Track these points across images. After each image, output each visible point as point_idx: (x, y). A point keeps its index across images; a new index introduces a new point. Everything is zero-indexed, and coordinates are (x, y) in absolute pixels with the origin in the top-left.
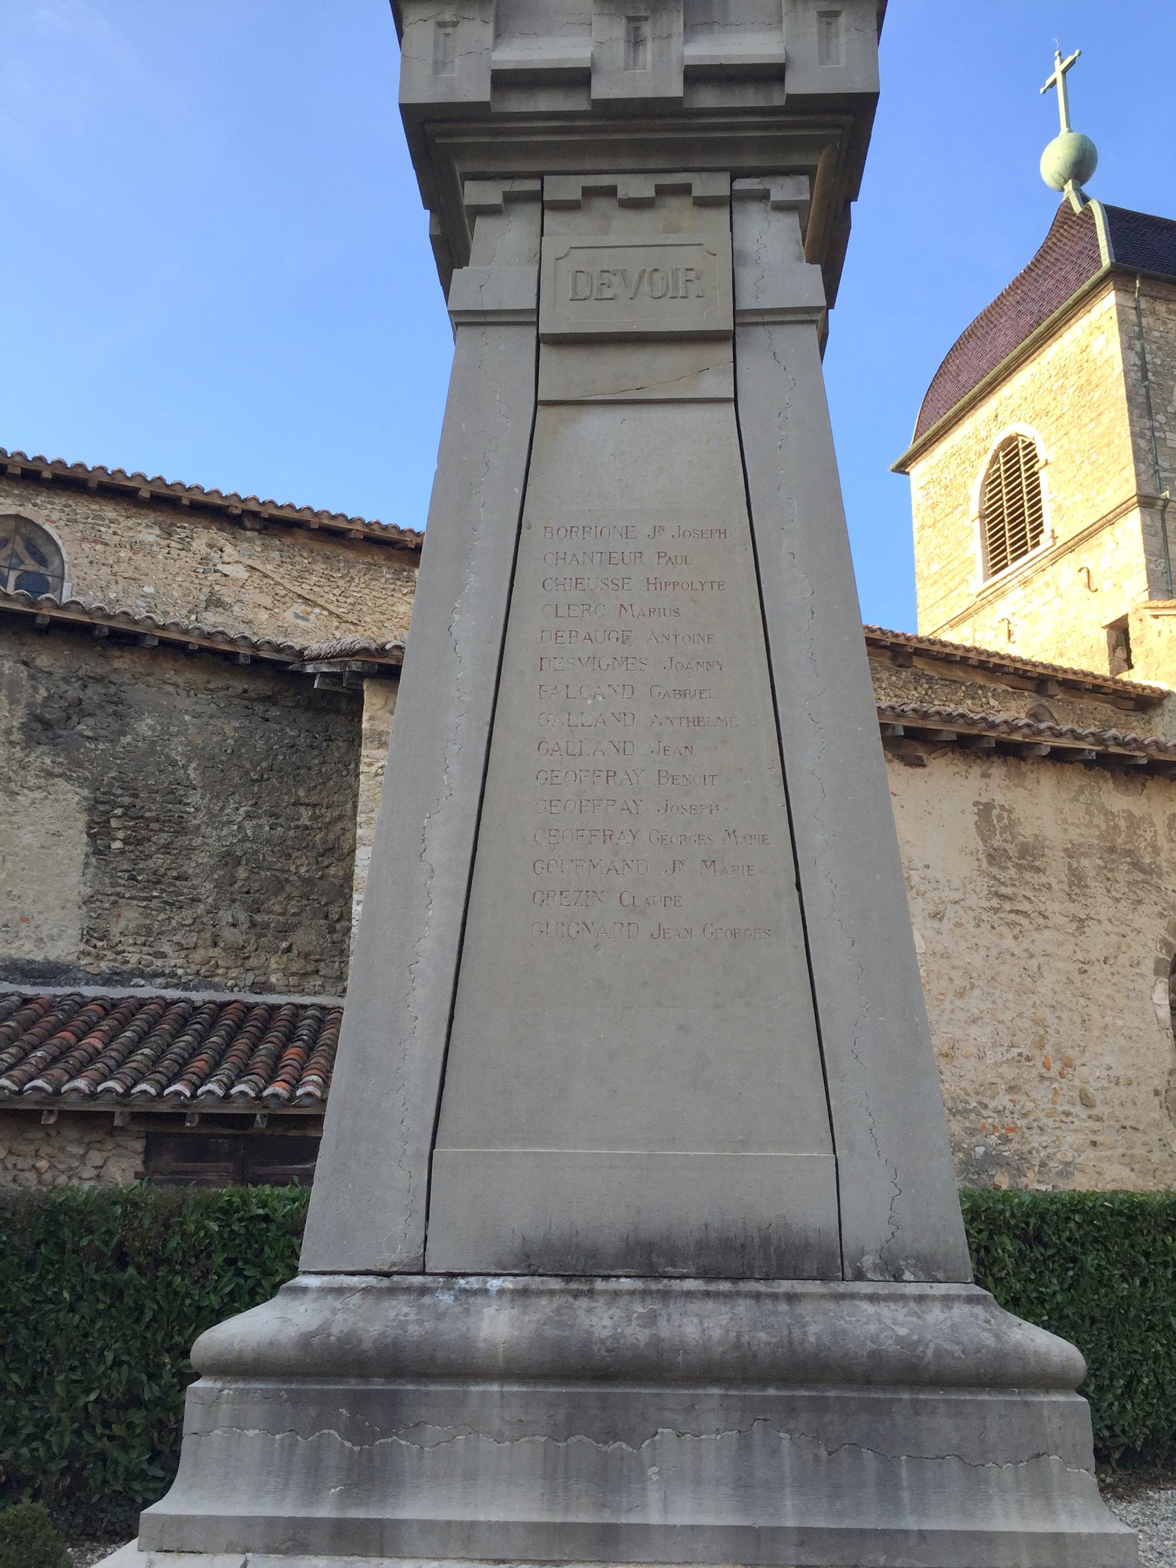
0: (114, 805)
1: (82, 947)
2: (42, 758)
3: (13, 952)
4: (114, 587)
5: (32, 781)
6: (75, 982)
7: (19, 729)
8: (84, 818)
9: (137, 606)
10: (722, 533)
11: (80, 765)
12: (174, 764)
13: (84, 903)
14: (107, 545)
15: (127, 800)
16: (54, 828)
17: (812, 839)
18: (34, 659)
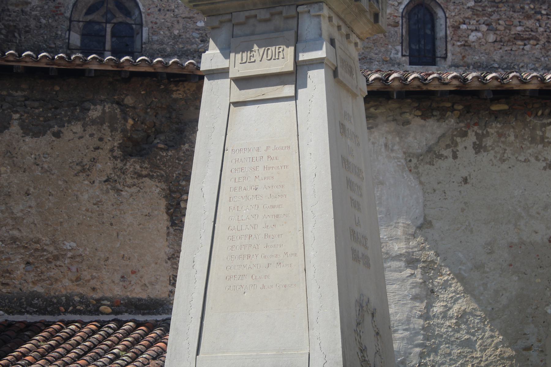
3: (128, 294)
4: (176, 26)
5: (129, 181)
7: (118, 147)
8: (163, 203)
9: (194, 38)
10: (289, 147)
11: (158, 167)
13: (169, 259)
16: (146, 211)
17: (311, 253)
18: (123, 100)
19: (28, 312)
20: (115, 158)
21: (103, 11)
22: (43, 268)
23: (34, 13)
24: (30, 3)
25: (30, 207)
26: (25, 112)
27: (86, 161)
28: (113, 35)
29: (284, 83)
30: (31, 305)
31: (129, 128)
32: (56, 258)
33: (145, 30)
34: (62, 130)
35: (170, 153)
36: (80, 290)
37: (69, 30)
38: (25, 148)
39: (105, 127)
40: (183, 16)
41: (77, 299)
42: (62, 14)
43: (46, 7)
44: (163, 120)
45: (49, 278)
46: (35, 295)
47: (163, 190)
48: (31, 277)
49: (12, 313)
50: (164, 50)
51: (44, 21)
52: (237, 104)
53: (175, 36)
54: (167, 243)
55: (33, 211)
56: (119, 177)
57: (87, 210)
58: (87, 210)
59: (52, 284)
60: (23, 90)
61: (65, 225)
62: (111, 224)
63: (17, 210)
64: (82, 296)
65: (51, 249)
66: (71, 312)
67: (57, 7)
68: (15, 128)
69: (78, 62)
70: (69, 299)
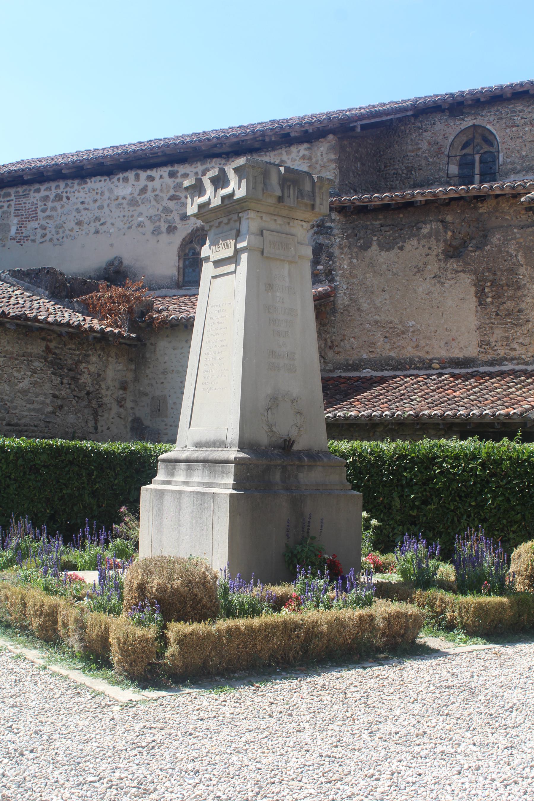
0: (485, 281)
1: (479, 349)
2: (453, 264)
4: (524, 149)
5: (449, 276)
6: (478, 366)
8: (473, 289)
11: (469, 264)
12: (511, 255)
14: (518, 126)
15: (491, 277)
16: (461, 296)
18: (445, 218)
19: (386, 370)
20: (440, 260)
21: (471, 147)
22: (395, 340)
23: (424, 155)
24: (421, 148)
25: (386, 299)
26: (381, 235)
27: (420, 264)
28: (481, 162)
29: (231, 263)
30: (388, 365)
31: (448, 238)
32: (403, 333)
33: (501, 155)
34: (405, 244)
35: (477, 253)
36: (419, 354)
37: (448, 164)
38: (381, 260)
39: (432, 239)
40: (529, 140)
41: (417, 359)
42: (443, 153)
43: (432, 149)
44: (474, 229)
45: (399, 346)
46: (390, 358)
47: (473, 280)
48: (387, 346)
49: (376, 371)
50: (515, 168)
51: (431, 160)
52: (214, 277)
53: (523, 156)
54: (476, 318)
55: (388, 302)
56: (443, 274)
57: (422, 299)
58: (422, 299)
59: (400, 350)
60: (380, 220)
61: (408, 310)
62: (438, 307)
63: (378, 302)
64: (420, 358)
65: (400, 327)
66: (413, 369)
67: (439, 149)
68: (375, 247)
69: (408, 197)
70: (412, 360)
